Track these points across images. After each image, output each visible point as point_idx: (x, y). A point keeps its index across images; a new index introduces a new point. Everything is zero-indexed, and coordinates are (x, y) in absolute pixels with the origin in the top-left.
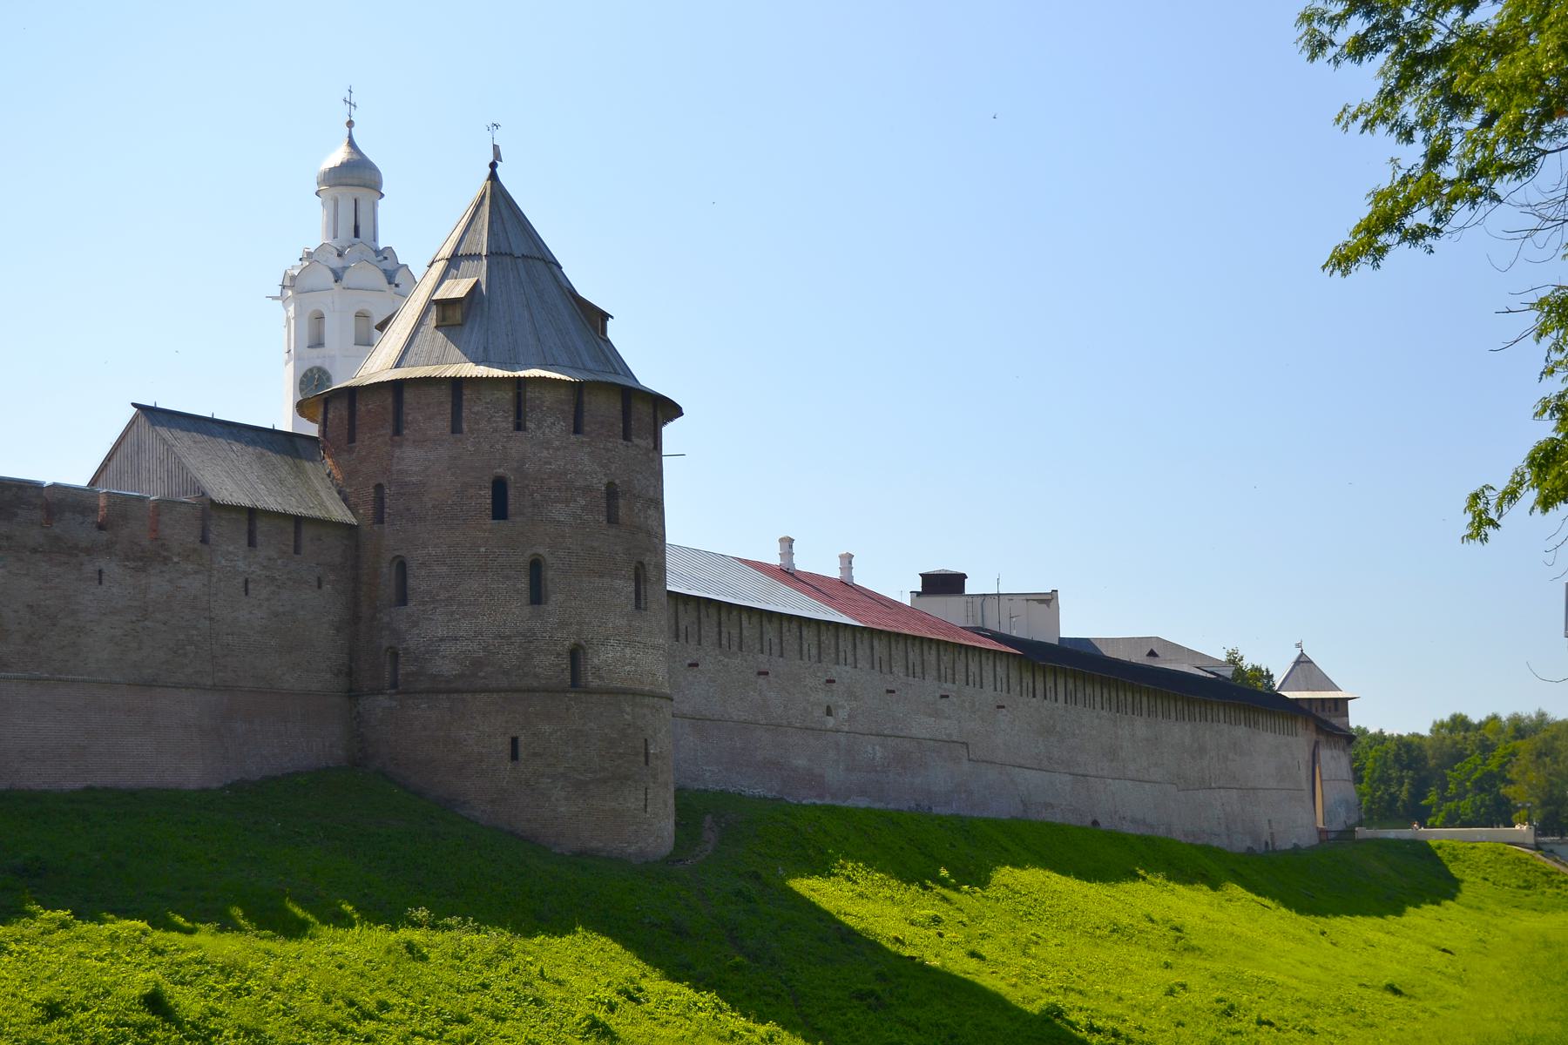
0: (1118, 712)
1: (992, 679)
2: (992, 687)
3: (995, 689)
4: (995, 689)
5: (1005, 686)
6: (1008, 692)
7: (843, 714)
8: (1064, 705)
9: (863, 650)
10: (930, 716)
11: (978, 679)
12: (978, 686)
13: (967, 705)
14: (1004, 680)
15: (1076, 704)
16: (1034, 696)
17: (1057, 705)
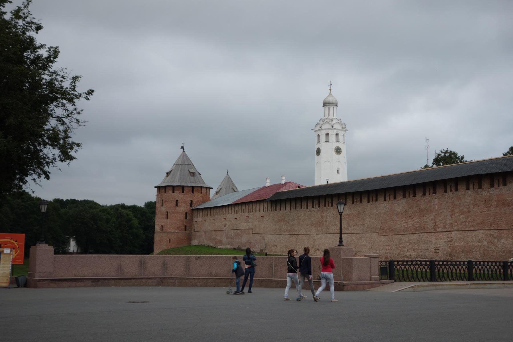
0: (325, 206)
1: (263, 208)
2: (263, 211)
3: (264, 211)
4: (264, 211)
5: (267, 210)
6: (267, 211)
7: (227, 226)
8: (289, 210)
9: (230, 209)
10: (245, 223)
11: (259, 209)
12: (259, 211)
13: (255, 217)
14: (267, 208)
15: (296, 209)
16: (276, 210)
17: (286, 211)
